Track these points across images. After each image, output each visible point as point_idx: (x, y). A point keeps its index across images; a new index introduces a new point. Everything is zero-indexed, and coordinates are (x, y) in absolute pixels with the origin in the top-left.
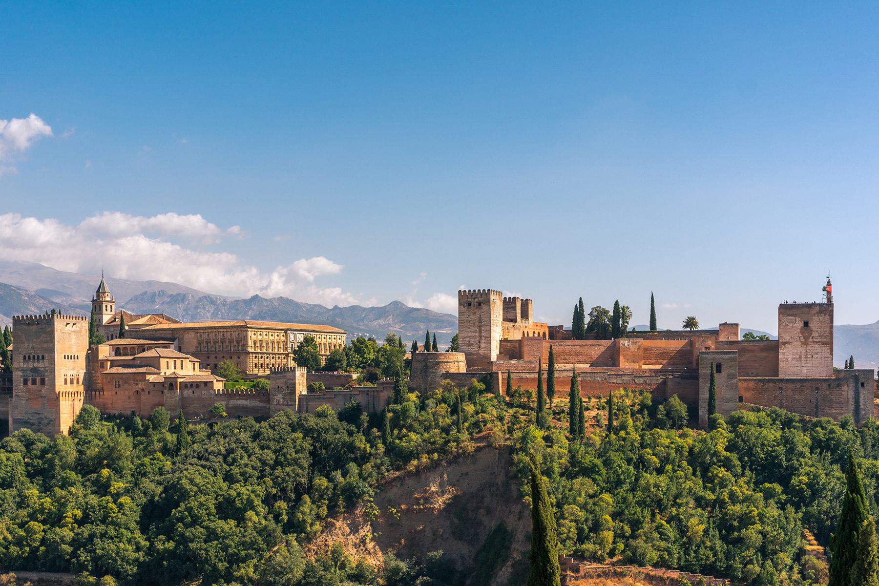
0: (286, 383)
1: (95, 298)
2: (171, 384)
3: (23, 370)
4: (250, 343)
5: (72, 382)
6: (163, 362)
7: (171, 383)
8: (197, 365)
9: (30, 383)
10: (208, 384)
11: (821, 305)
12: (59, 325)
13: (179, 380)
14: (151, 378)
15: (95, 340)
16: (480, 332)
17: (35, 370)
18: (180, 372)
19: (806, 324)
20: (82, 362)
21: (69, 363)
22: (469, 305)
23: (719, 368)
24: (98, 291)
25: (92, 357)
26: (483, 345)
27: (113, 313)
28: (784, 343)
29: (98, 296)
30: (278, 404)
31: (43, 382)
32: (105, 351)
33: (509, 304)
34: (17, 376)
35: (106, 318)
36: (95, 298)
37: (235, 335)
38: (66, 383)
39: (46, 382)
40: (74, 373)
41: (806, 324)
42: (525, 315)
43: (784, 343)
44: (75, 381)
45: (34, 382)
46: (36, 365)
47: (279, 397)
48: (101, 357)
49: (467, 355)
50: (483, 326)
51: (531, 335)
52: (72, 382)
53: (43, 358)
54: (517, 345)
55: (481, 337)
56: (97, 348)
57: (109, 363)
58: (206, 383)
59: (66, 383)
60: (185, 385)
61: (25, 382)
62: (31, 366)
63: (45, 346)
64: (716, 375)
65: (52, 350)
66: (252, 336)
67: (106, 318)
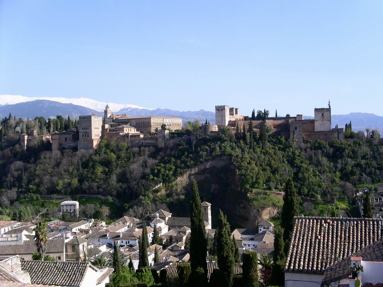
0: (162, 135)
1: (105, 110)
2: (127, 136)
3: (82, 132)
4: (152, 123)
5: (97, 136)
6: (125, 129)
7: (127, 135)
8: (136, 130)
9: (84, 136)
10: (139, 136)
11: (327, 109)
12: (93, 118)
13: (130, 135)
14: (121, 134)
15: (104, 122)
16: (222, 118)
17: (86, 132)
18: (130, 132)
19: (323, 115)
20: (100, 130)
21: (96, 130)
22: (219, 110)
23: (296, 129)
24: (106, 108)
25: (103, 127)
26: (223, 122)
27: (111, 114)
28: (316, 121)
29: (106, 109)
30: (160, 142)
31: (88, 136)
32: (107, 126)
33: (231, 110)
34: (80, 134)
35: (109, 116)
36: (105, 110)
37: (147, 121)
38: (95, 136)
39: (89, 136)
40: (98, 133)
41: (323, 115)
42: (236, 113)
43: (316, 121)
44: (98, 136)
45: (86, 136)
46: (86, 131)
47: (160, 139)
48: (106, 128)
49: (218, 125)
50: (223, 117)
51: (238, 119)
52: (97, 136)
53: (88, 128)
54: (234, 122)
55: (222, 120)
56: (105, 125)
57: (108, 129)
58: (138, 136)
59: (95, 136)
60: (132, 136)
61: (83, 136)
62: (85, 131)
63: (89, 125)
64: (295, 131)
65: (91, 126)
66: (153, 121)
67: (109, 116)
